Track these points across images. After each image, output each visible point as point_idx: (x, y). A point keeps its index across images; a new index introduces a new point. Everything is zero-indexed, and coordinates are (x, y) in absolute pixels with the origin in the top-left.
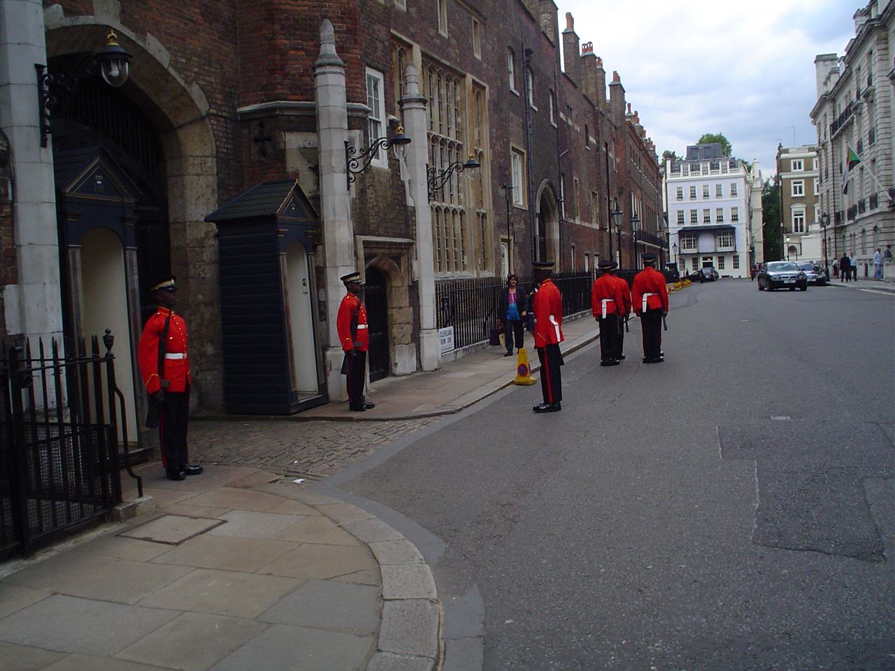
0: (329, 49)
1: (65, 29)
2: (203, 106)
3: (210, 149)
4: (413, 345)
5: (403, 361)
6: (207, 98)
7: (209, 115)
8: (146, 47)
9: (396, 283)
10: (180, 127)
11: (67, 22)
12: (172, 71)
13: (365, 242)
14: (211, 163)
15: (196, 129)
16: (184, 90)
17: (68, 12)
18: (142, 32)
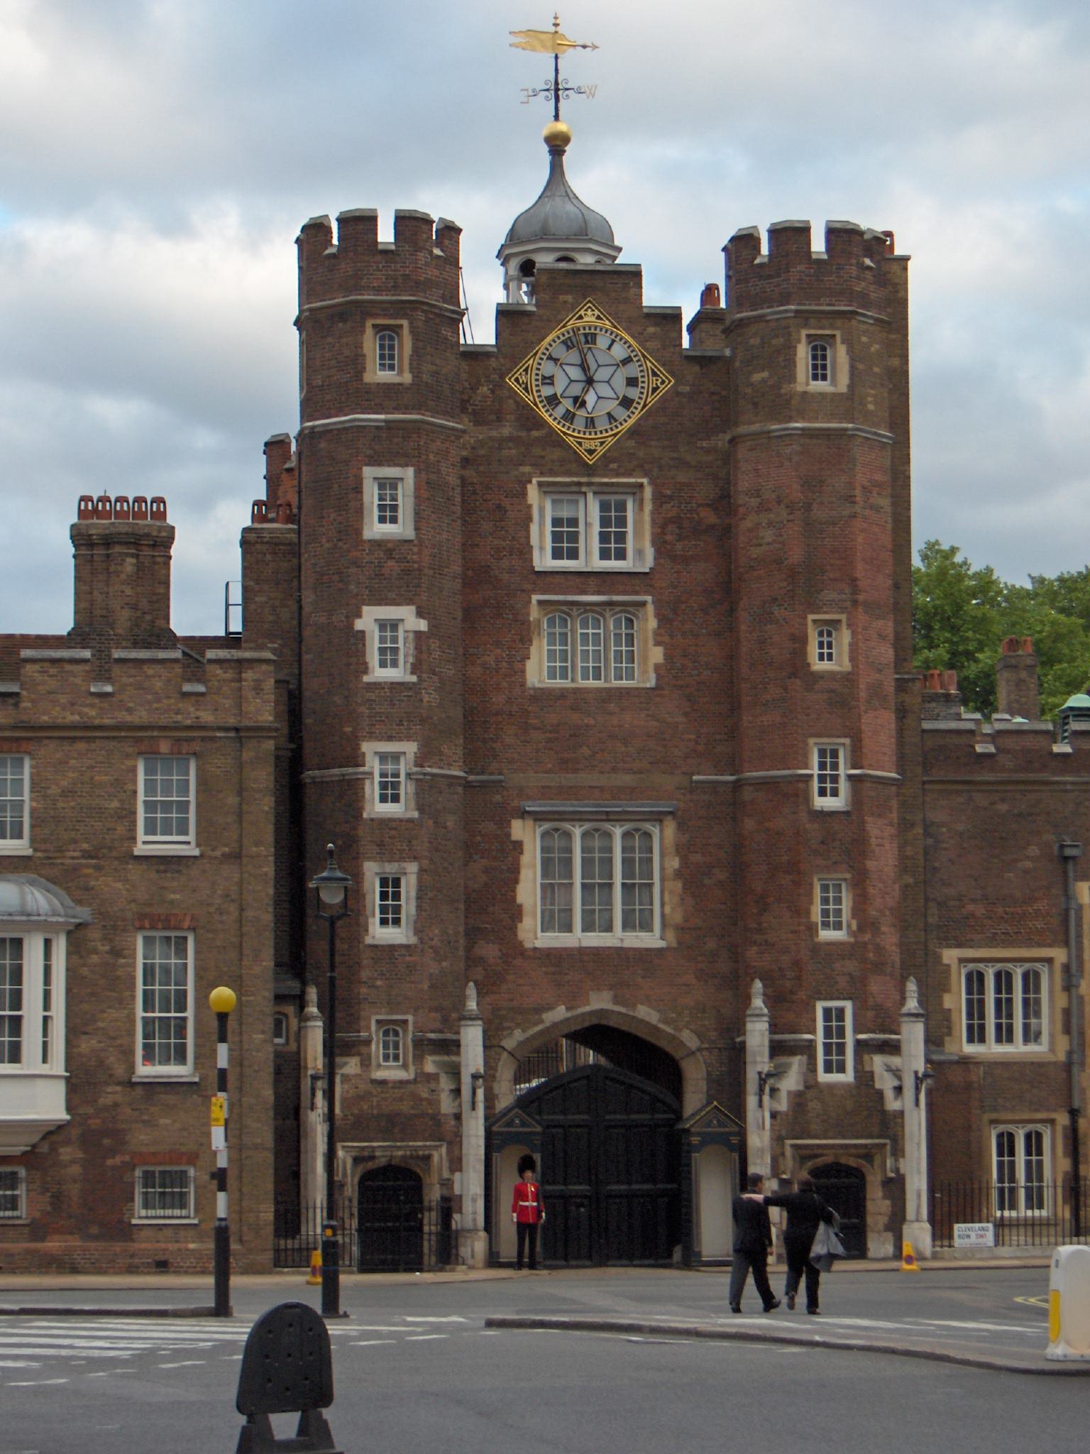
0: (758, 1002)
1: (568, 1019)
3: (702, 1073)
4: (890, 1235)
5: (879, 1245)
6: (699, 1037)
7: (700, 1050)
8: (636, 1014)
9: (870, 1178)
11: (569, 1014)
12: (661, 1026)
13: (792, 1146)
14: (703, 1085)
16: (674, 1037)
17: (568, 1009)
18: (634, 1007)
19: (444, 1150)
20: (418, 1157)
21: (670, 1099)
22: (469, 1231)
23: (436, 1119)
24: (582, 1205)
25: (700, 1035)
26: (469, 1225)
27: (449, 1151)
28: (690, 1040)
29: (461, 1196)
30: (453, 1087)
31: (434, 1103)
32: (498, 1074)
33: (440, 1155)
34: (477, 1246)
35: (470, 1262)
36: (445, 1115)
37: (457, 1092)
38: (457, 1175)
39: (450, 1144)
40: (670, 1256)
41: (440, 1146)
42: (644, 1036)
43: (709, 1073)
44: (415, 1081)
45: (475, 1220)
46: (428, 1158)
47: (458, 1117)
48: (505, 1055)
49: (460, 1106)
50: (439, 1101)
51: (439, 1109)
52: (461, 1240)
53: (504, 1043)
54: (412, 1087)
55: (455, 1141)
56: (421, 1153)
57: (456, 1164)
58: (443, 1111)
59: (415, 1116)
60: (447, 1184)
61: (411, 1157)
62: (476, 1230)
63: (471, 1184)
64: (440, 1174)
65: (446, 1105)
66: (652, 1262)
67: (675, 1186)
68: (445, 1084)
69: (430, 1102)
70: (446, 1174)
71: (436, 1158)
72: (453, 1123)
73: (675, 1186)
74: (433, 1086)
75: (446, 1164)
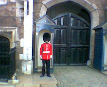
2: (95, 6)
3: (98, 15)
7: (97, 9)
10: (92, 12)
14: (98, 19)
15: (94, 12)
16: (91, 5)
19: (17, 30)
20: (7, 32)
21: (86, 22)
22: (26, 61)
23: (14, 19)
24: (64, 49)
25: (97, 5)
26: (25, 58)
27: (19, 31)
28: (95, 6)
29: (23, 47)
30: (21, 7)
31: (14, 12)
32: (41, 11)
33: (15, 32)
34: (27, 68)
35: (26, 73)
36: (17, 17)
37: (23, 9)
38: (22, 39)
39: (19, 28)
40: (86, 62)
41: (15, 29)
42: (82, 5)
43: (100, 16)
44: (7, 5)
45: (28, 57)
46: (11, 33)
47: (22, 18)
48: (43, 5)
49: (24, 14)
50: (15, 12)
51: (15, 15)
52: (23, 64)
53: (43, 2)
54: (5, 7)
55: (21, 27)
56: (8, 31)
57: (21, 36)
58: (17, 16)
59: (6, 17)
60: (18, 43)
61: (4, 32)
62: (28, 60)
63: (26, 43)
64: (15, 39)
65: (18, 14)
66: (81, 64)
67: (88, 45)
68: (18, 6)
69: (12, 12)
70: (17, 39)
71: (14, 33)
72: (20, 20)
73: (88, 45)
74: (13, 6)
75: (17, 36)
